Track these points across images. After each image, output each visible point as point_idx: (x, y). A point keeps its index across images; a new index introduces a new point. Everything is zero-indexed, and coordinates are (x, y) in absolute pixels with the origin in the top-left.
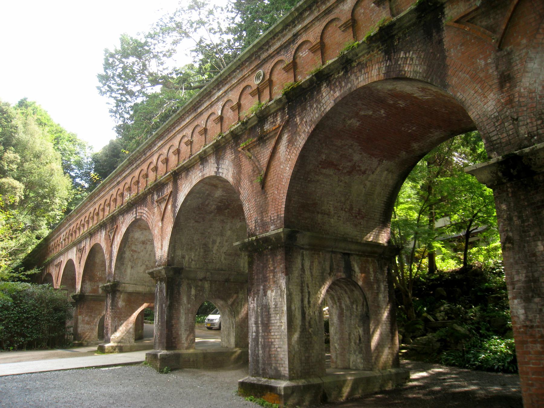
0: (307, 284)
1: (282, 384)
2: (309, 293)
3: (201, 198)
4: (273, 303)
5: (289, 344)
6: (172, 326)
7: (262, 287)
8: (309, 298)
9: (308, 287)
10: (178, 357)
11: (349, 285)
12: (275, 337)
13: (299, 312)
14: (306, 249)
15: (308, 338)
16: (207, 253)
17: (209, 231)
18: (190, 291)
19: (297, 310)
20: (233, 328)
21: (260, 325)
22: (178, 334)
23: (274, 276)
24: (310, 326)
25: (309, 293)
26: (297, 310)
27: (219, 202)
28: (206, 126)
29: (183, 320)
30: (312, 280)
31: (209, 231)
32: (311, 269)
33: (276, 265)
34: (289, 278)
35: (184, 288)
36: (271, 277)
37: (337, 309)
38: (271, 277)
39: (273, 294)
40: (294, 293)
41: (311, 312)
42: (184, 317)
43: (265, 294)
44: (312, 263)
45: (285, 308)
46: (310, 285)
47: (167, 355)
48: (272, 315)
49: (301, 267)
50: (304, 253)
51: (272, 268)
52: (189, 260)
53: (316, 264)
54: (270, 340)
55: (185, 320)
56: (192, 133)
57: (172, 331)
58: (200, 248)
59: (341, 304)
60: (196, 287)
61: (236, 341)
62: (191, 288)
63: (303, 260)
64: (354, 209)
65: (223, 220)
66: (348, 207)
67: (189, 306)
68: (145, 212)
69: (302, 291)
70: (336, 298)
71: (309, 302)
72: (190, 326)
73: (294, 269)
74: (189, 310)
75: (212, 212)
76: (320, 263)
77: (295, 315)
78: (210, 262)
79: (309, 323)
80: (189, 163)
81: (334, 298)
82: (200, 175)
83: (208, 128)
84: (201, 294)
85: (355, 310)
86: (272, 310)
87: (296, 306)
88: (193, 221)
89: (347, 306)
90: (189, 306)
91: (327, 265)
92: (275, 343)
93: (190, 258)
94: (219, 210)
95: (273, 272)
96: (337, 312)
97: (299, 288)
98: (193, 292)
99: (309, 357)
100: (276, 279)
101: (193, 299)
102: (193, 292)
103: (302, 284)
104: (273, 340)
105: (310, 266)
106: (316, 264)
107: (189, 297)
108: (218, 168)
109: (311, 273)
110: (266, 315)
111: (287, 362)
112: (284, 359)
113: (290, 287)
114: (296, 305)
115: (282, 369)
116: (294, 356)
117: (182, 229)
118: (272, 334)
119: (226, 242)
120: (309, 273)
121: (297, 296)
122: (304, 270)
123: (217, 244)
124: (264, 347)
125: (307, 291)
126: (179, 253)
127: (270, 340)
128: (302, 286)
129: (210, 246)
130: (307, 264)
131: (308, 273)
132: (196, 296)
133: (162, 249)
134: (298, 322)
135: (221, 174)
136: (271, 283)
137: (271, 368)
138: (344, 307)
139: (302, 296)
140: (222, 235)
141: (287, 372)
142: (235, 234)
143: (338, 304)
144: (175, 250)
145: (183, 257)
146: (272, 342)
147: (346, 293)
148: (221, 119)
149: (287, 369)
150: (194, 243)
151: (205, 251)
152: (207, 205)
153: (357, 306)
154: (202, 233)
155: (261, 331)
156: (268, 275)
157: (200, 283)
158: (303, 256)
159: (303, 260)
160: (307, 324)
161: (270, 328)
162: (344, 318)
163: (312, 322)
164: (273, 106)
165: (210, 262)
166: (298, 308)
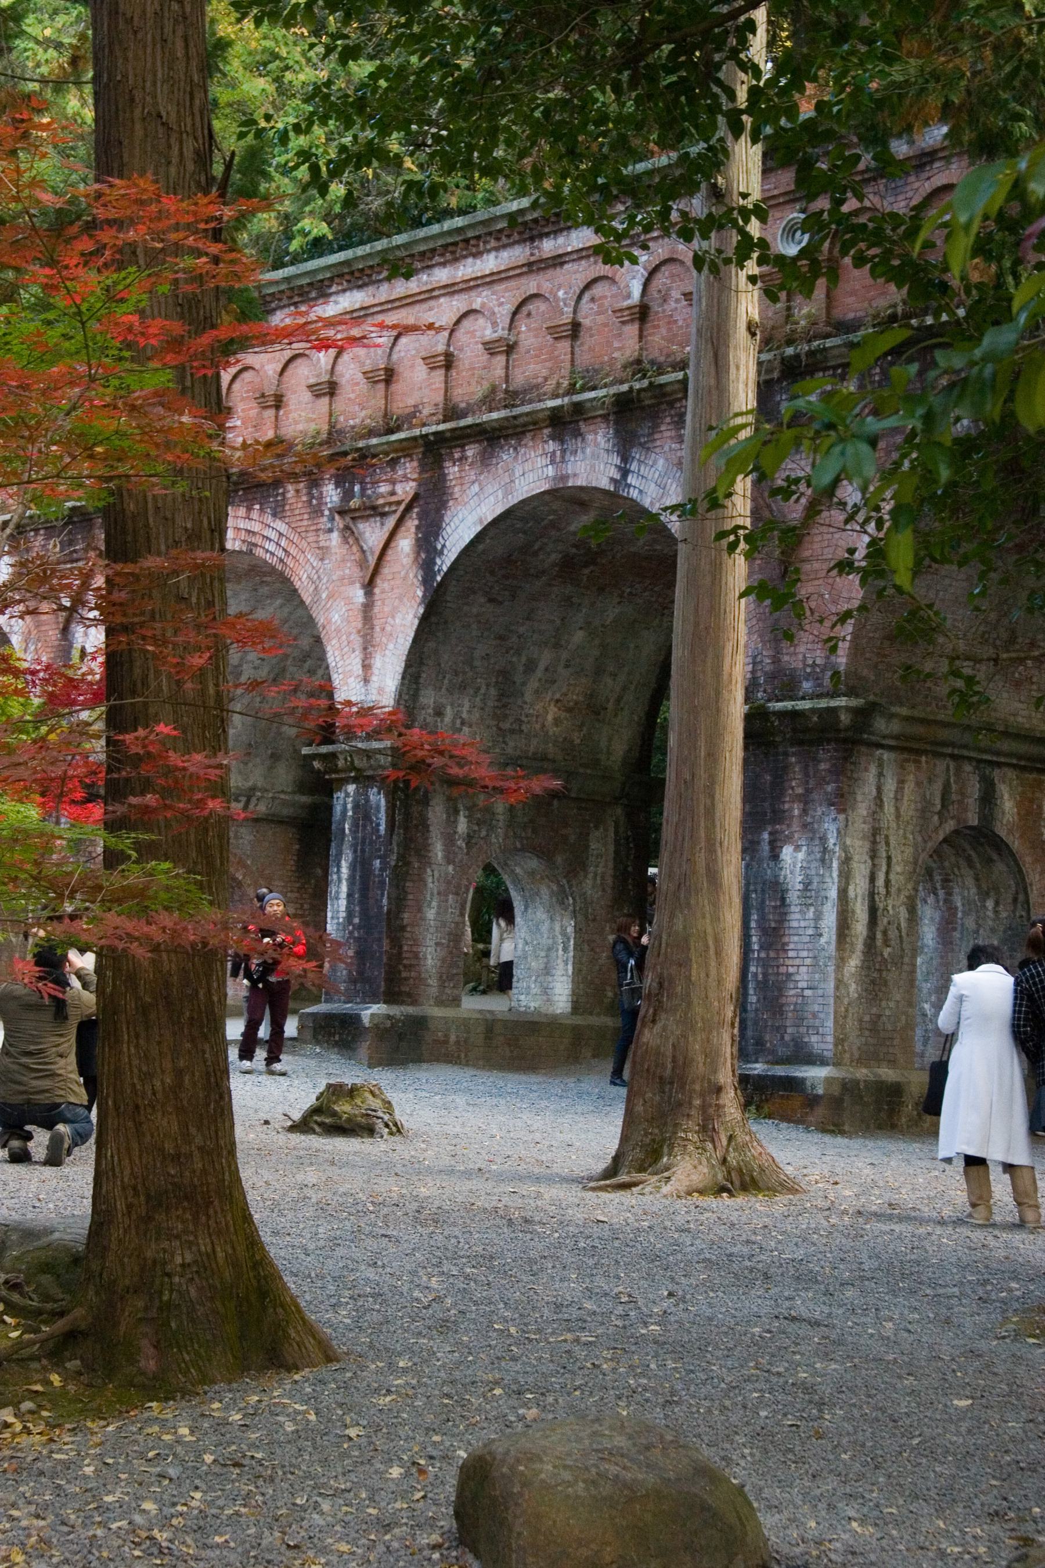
0: (887, 837)
1: (816, 1074)
2: (889, 858)
3: (525, 533)
4: (800, 879)
5: (839, 983)
6: (403, 928)
7: (766, 836)
8: (887, 873)
9: (888, 844)
10: (419, 1023)
11: (982, 845)
12: (797, 962)
13: (863, 904)
14: (890, 748)
15: (880, 971)
16: (505, 700)
17: (521, 630)
18: (456, 822)
19: (859, 899)
20: (565, 949)
21: (753, 932)
22: (416, 956)
23: (805, 812)
24: (886, 943)
25: (889, 858)
26: (859, 899)
27: (575, 546)
28: (575, 312)
29: (431, 914)
30: (899, 828)
31: (521, 630)
32: (897, 799)
33: (812, 783)
34: (847, 820)
35: (436, 813)
36: (796, 812)
37: (937, 908)
38: (796, 812)
39: (801, 856)
40: (856, 858)
41: (890, 908)
42: (434, 904)
43: (775, 856)
44: (901, 782)
45: (833, 893)
46: (892, 841)
47: (389, 1017)
48: (793, 909)
49: (874, 792)
50: (885, 757)
51: (800, 791)
52: (453, 722)
53: (909, 786)
54: (783, 970)
55: (438, 913)
56: (515, 313)
57: (401, 947)
58: (488, 685)
59: (949, 894)
60: (471, 809)
61: (574, 993)
62: (456, 812)
63: (880, 775)
64: (1020, 640)
65: (569, 598)
66: (1004, 635)
67: (451, 868)
68: (273, 535)
69: (873, 855)
70: (937, 878)
71: (887, 883)
72: (450, 934)
73: (859, 798)
74: (449, 883)
75: (543, 572)
76: (918, 784)
77: (853, 912)
78: (512, 731)
79: (885, 933)
80: (506, 424)
81: (931, 876)
82: (550, 471)
83: (586, 322)
84: (483, 833)
85: (990, 914)
86: (793, 897)
87: (858, 890)
88: (482, 600)
89: (967, 902)
90: (451, 868)
91: (936, 790)
92: (798, 978)
93: (457, 715)
94: (568, 567)
95: (805, 800)
96: (937, 916)
97: (867, 845)
98: (462, 825)
99: (879, 1016)
100: (809, 820)
101: (460, 848)
102: (462, 825)
103: (874, 835)
104: (791, 970)
105: (896, 792)
106: (909, 786)
107: (450, 840)
108: (625, 472)
109: (897, 809)
110: (775, 907)
111: (830, 1023)
112: (822, 1016)
113: (848, 842)
114: (859, 888)
115: (814, 1039)
116: (847, 1011)
117: (446, 622)
118: (791, 954)
119: (567, 666)
120: (892, 810)
121: (863, 866)
122: (881, 801)
123: (539, 673)
124: (763, 986)
125: (884, 855)
126: (428, 698)
127: (783, 970)
128: (874, 842)
129: (518, 679)
130: (890, 785)
131: (889, 808)
132: (469, 838)
133: (366, 681)
134: (860, 927)
135: (634, 494)
136: (796, 826)
137: (782, 1038)
138: (959, 904)
139: (874, 865)
140: (557, 646)
141: (831, 1047)
142: (597, 642)
143: (941, 893)
144: (417, 690)
145: (439, 713)
146: (789, 975)
147: (971, 865)
148: (642, 313)
149: (830, 1039)
150: (472, 667)
151: (502, 695)
152: (535, 554)
153: (997, 903)
154: (501, 638)
155: (756, 947)
156: (787, 806)
157: (481, 800)
158: (880, 766)
159: (880, 775)
160: (879, 936)
161: (786, 939)
162: (956, 935)
163: (893, 934)
164: (836, 352)
165: (512, 731)
166: (863, 895)
